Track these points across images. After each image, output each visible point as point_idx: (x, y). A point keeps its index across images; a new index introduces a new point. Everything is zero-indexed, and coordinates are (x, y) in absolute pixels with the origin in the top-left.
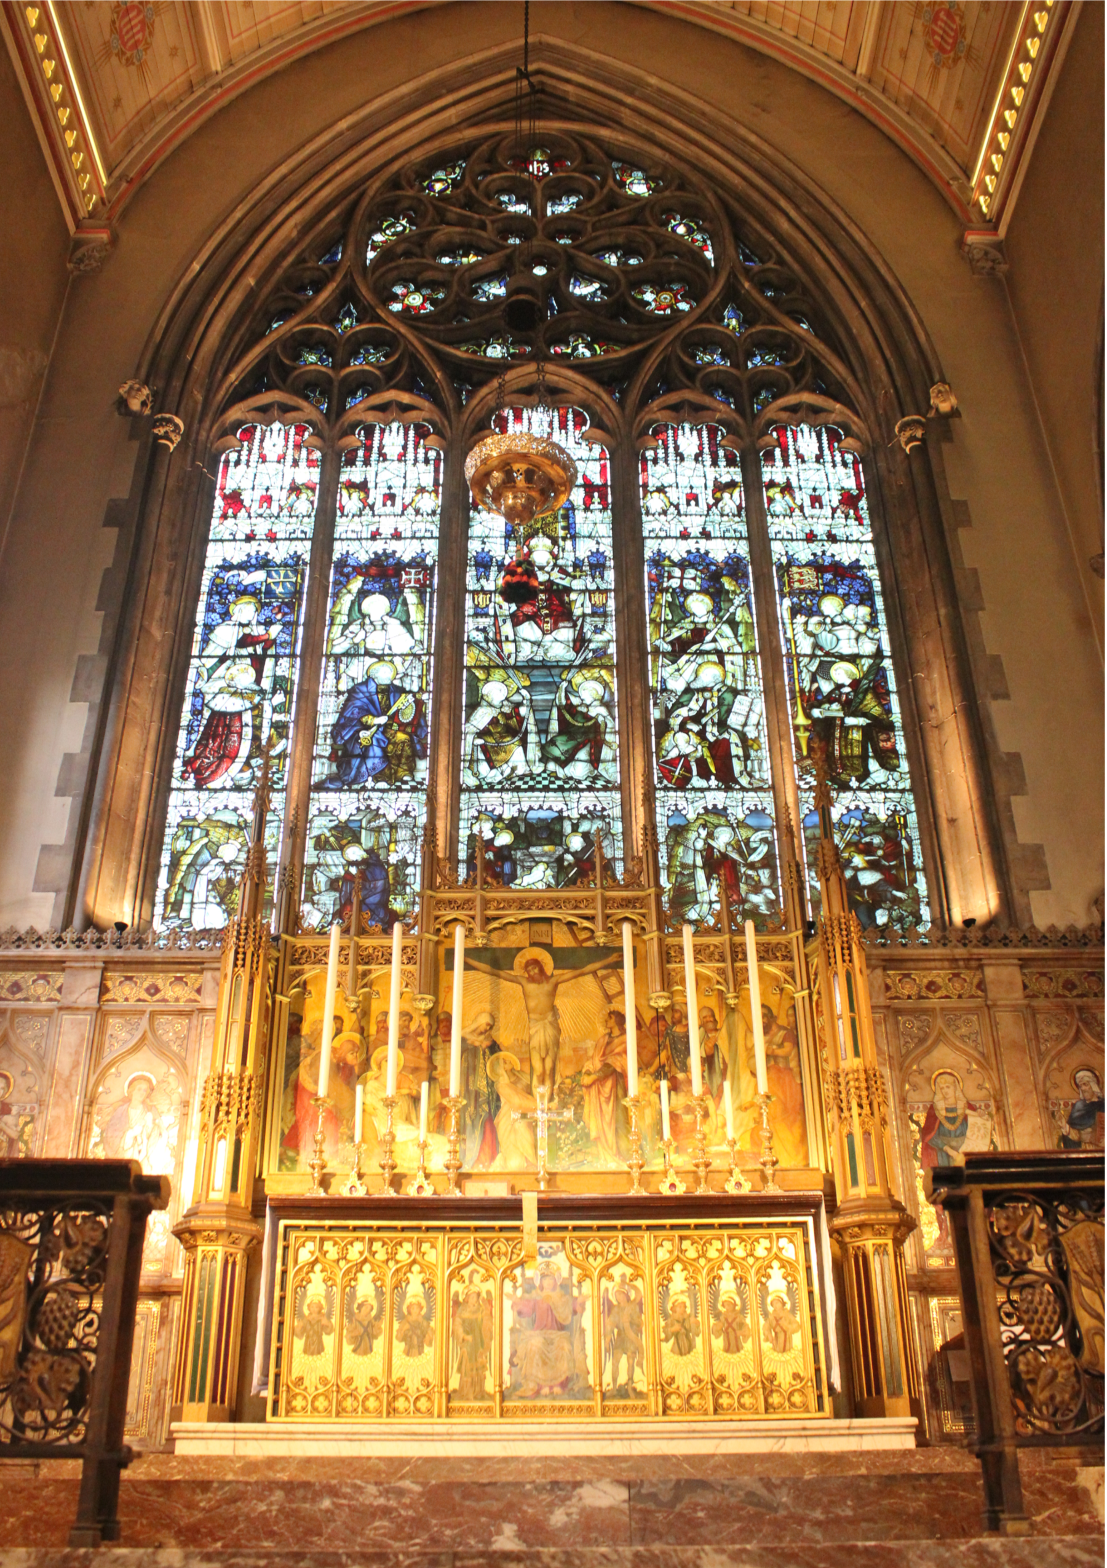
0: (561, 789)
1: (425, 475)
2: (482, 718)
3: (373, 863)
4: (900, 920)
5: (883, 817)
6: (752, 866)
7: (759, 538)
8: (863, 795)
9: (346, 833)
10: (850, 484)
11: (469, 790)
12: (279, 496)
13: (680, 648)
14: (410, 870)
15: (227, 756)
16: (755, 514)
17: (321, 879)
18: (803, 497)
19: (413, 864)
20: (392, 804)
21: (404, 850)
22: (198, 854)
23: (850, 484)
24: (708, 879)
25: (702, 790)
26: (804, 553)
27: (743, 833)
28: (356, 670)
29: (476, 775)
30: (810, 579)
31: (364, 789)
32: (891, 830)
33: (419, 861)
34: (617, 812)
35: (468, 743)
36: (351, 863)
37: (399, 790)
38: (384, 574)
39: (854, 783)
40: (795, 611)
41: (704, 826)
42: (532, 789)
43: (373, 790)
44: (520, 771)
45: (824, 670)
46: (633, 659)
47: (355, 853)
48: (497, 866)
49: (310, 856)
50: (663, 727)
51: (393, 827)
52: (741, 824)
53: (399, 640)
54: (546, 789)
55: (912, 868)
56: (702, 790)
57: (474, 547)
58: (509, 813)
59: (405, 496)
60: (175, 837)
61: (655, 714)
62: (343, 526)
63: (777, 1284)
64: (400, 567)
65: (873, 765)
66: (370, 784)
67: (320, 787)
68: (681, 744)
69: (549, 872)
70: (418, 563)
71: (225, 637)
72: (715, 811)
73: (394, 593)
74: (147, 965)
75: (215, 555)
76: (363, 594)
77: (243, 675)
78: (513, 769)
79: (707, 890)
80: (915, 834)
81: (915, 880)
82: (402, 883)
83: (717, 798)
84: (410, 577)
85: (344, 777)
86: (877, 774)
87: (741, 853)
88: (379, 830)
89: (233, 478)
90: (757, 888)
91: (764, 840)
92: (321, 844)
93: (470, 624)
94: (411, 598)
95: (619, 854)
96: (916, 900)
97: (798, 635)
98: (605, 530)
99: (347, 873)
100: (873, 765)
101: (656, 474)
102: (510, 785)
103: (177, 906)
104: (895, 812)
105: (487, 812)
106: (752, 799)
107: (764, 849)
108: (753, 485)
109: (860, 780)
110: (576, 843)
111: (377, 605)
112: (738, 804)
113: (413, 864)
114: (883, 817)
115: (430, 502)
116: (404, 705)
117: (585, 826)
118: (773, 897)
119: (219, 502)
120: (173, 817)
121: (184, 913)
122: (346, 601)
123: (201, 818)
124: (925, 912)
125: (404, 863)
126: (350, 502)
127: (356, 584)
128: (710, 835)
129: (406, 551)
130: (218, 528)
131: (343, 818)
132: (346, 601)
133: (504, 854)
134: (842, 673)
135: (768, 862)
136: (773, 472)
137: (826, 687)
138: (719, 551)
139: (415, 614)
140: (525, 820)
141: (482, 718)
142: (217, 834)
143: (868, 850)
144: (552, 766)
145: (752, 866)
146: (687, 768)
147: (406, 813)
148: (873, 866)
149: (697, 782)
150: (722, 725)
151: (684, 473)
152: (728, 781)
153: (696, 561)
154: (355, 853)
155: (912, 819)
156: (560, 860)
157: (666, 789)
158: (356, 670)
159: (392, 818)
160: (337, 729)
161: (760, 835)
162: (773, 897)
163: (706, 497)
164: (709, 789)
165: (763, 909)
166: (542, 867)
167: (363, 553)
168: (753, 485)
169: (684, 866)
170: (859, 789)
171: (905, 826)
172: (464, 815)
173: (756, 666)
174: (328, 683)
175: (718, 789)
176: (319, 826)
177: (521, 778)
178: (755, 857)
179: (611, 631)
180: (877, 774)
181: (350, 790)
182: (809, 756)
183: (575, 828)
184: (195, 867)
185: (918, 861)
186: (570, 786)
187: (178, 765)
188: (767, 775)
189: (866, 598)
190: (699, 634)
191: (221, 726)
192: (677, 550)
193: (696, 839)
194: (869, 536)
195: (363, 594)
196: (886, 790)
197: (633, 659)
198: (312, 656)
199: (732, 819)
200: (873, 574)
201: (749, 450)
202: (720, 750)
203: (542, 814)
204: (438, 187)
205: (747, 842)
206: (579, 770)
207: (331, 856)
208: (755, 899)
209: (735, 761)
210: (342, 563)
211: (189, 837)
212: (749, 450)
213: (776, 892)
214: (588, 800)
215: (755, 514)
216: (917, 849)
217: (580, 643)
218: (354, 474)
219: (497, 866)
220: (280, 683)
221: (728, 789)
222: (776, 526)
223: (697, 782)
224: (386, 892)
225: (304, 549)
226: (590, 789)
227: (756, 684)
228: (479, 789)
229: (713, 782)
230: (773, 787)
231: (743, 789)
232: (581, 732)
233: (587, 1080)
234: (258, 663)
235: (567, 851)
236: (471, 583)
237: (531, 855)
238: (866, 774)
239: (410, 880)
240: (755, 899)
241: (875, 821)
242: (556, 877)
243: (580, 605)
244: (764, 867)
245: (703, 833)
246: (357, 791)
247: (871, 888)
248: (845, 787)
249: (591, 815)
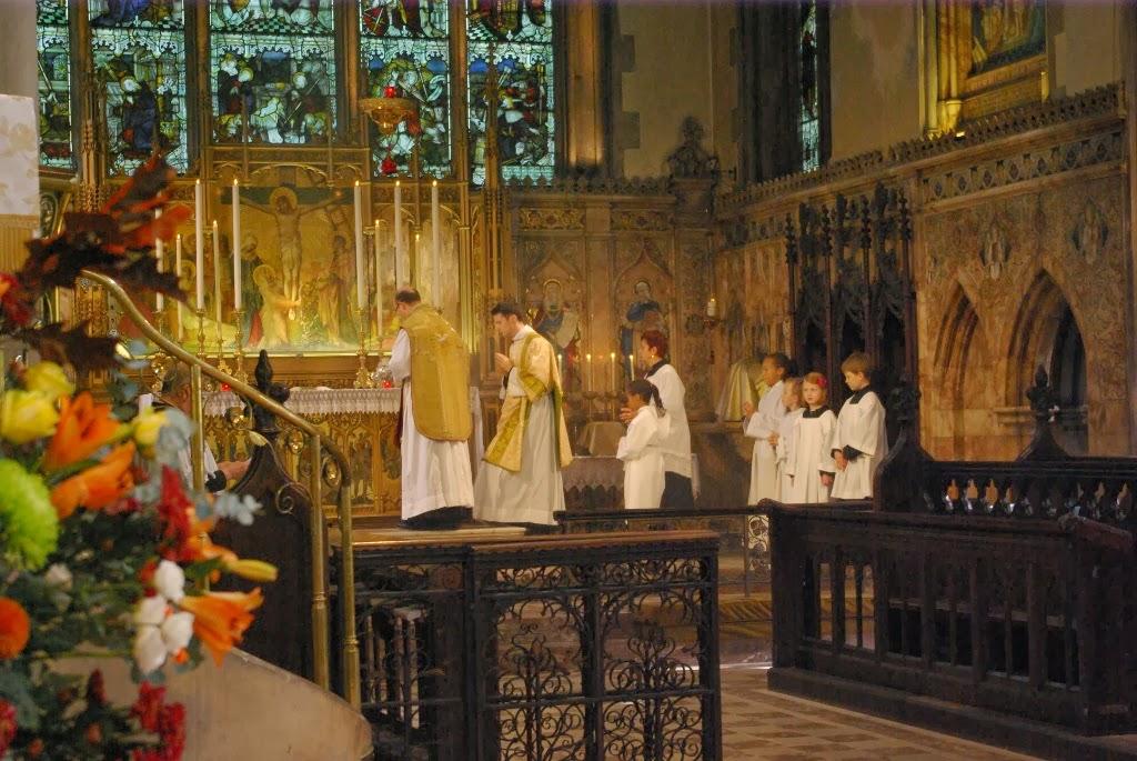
0: (288, 33)
3: (145, 94)
4: (533, 151)
5: (528, 66)
6: (429, 104)
8: (515, 46)
9: (123, 65)
11: (216, 30)
14: (175, 101)
19: (177, 96)
25: (396, 38)
27: (425, 76)
29: (222, 17)
31: (132, 27)
32: (533, 77)
33: (183, 92)
34: (331, 55)
37: (161, 29)
39: (509, 36)
41: (396, 69)
42: (266, 33)
43: (140, 28)
44: (257, 15)
47: (130, 85)
48: (237, 98)
51: (159, 62)
52: (424, 68)
54: (277, 33)
55: (546, 110)
56: (396, 38)
58: (248, 53)
65: (526, 20)
66: (137, 22)
67: (96, 24)
69: (280, 105)
72: (407, 57)
78: (251, 14)
80: (550, 81)
81: (546, 120)
82: (169, 111)
83: (407, 46)
86: (528, 29)
87: (422, 94)
88: (147, 64)
90: (433, 123)
91: (440, 83)
95: (333, 91)
96: (545, 135)
99: (126, 101)
100: (526, 20)
102: (249, 28)
104: (538, 62)
105: (230, 55)
106: (433, 48)
107: (439, 91)
109: (515, 33)
110: (301, 81)
112: (424, 51)
113: (177, 96)
114: (528, 66)
117: (307, 67)
118: (443, 130)
124: (551, 145)
125: (169, 95)
128: (400, 77)
131: (118, 52)
133: (246, 88)
135: (441, 101)
140: (262, 59)
143: (515, 94)
144: (281, 12)
145: (429, 104)
146: (385, 18)
147: (168, 50)
148: (518, 107)
149: (392, 31)
152: (415, 31)
154: (130, 85)
155: (550, 67)
156: (288, 95)
157: (369, 36)
159: (157, 53)
161: (437, 78)
162: (443, 130)
164: (401, 37)
165: (436, 140)
166: (275, 101)
170: (513, 41)
171: (544, 74)
172: (214, 53)
175: (408, 37)
177: (258, 21)
178: (432, 98)
180: (528, 29)
181: (121, 27)
182: (478, 10)
185: (550, 104)
186: (294, 31)
188: (446, 27)
196: (532, 43)
199: (417, 63)
203: (274, 55)
205: (427, 84)
206: (302, 17)
208: (432, 131)
209: (421, 11)
213: (446, 126)
214: (309, 44)
216: (551, 94)
219: (237, 98)
221: (415, 38)
223: (392, 31)
224: (157, 119)
226: (311, 34)
228: (224, 31)
229: (405, 31)
230: (449, 38)
231: (427, 38)
235: (294, 88)
237: (267, 90)
238: (520, 27)
239: (175, 109)
240: (432, 131)
241: (521, 70)
242: (286, 110)
244: (438, 105)
245: (395, 76)
246: (128, 29)
247: (515, 125)
248: (503, 39)
249: (313, 57)
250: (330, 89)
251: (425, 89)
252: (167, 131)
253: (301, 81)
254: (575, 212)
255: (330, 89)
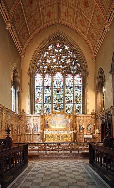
1: (50, 79)
2: (54, 99)
3: (48, 108)
7: (74, 84)
9: (46, 106)
10: (81, 79)
12: (40, 80)
13: (68, 93)
15: (38, 101)
16: (74, 82)
17: (45, 110)
18: (77, 81)
20: (49, 105)
21: (50, 108)
23: (81, 79)
26: (76, 85)
28: (46, 95)
30: (77, 88)
32: (80, 106)
35: (54, 101)
38: (48, 87)
40: (76, 90)
45: (77, 95)
46: (64, 94)
49: (44, 108)
50: (66, 99)
53: (49, 92)
57: (54, 85)
59: (49, 80)
61: (66, 98)
62: (45, 83)
63: (70, 135)
64: (49, 87)
68: (67, 100)
70: (50, 86)
71: (37, 92)
73: (48, 89)
74: (36, 116)
75: (36, 85)
76: (46, 89)
77: (38, 95)
79: (68, 110)
83: (70, 104)
84: (49, 87)
85: (46, 103)
89: (36, 79)
92: (45, 107)
93: (54, 91)
94: (49, 89)
97: (75, 92)
98: (63, 84)
101: (66, 79)
106: (72, 104)
108: (74, 80)
111: (47, 90)
112: (71, 105)
115: (51, 81)
116: (49, 97)
119: (35, 81)
120: (35, 105)
122: (45, 89)
126: (45, 81)
127: (46, 88)
129: (49, 85)
130: (36, 83)
132: (45, 89)
134: (78, 95)
136: (75, 78)
137: (77, 96)
138: (71, 85)
139: (50, 91)
141: (54, 99)
142: (38, 107)
143: (78, 108)
150: (70, 99)
151: (69, 78)
152: (70, 103)
153: (69, 86)
158: (46, 95)
160: (45, 99)
163: (70, 81)
167: (46, 85)
168: (74, 80)
173: (73, 95)
174: (44, 96)
176: (45, 106)
179: (63, 92)
187: (35, 102)
189: (81, 89)
190: (69, 92)
191: (38, 99)
192: (68, 85)
193: (68, 107)
194: (81, 84)
195: (46, 89)
197: (64, 94)
198: (43, 94)
200: (81, 87)
201: (74, 76)
202: (70, 101)
204: (50, 48)
207: (45, 108)
210: (45, 86)
212: (74, 76)
215: (74, 82)
217: (61, 93)
218: (45, 78)
220: (41, 96)
222: (75, 83)
225: (42, 85)
227: (72, 96)
232: (61, 99)
234: (40, 94)
236: (54, 88)
243: (61, 90)
250: (63, 108)
251: (71, 108)
252: (50, 111)
253: (60, 107)
254: (83, 117)
255: (63, 108)
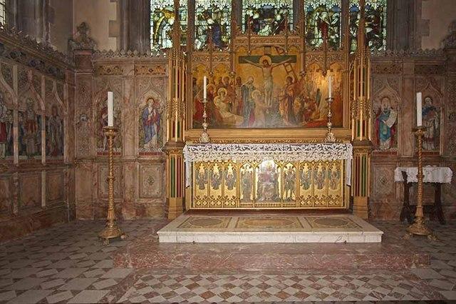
5: (375, 8)
6: (332, 26)
14: (228, 27)
22: (162, 22)
24: (318, 30)
27: (330, 14)
34: (291, 6)
36: (209, 25)
41: (318, 11)
47: (210, 21)
51: (222, 12)
52: (330, 11)
55: (382, 27)
60: (154, 16)
82: (225, 32)
87: (329, 21)
90: (333, 34)
91: (337, 17)
95: (292, 22)
103: (157, 40)
107: (337, 20)
110: (278, 17)
114: (375, 8)
117: (281, 12)
121: (160, 43)
123: (161, 9)
124: (384, 42)
125: (225, 25)
128: (320, 15)
131: (206, 9)
133: (256, 21)
135: (337, 25)
140: (263, 9)
142: (167, 15)
145: (332, 26)
147: (226, 7)
148: (370, 26)
154: (210, 21)
155: (385, 8)
156: (274, 23)
159: (221, 9)
161: (336, 15)
165: (334, 41)
166: (268, 26)
169: (311, 26)
171: (382, 11)
172: (244, 7)
183: (278, 12)
184: (162, 27)
185: (385, 24)
203: (268, 7)
208: (333, 37)
211: (158, 16)
213: (339, 35)
216: (385, 20)
224: (220, 35)
233: (280, 99)
237: (265, 22)
240: (333, 37)
241: (373, 9)
244: (336, 26)
245: (318, 14)
